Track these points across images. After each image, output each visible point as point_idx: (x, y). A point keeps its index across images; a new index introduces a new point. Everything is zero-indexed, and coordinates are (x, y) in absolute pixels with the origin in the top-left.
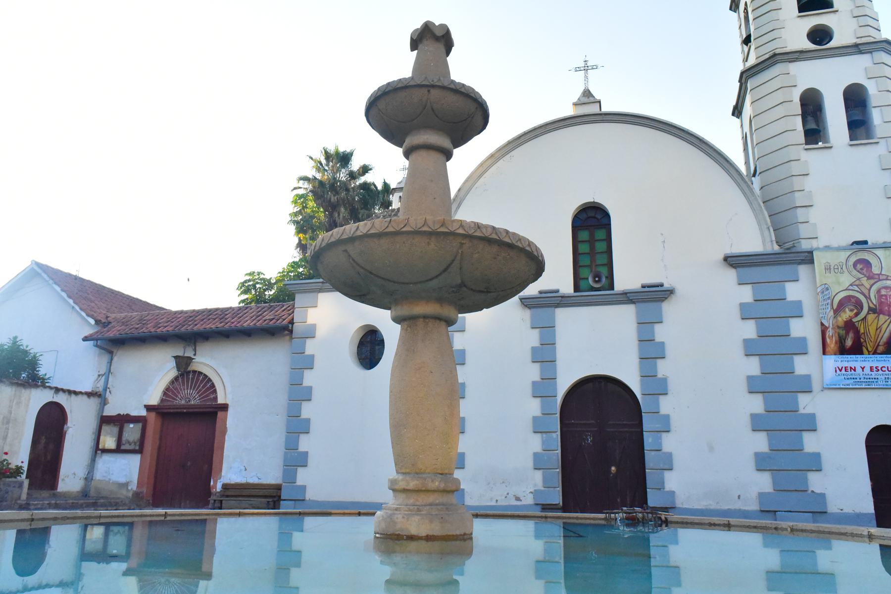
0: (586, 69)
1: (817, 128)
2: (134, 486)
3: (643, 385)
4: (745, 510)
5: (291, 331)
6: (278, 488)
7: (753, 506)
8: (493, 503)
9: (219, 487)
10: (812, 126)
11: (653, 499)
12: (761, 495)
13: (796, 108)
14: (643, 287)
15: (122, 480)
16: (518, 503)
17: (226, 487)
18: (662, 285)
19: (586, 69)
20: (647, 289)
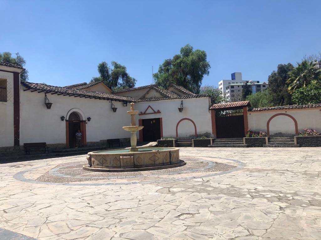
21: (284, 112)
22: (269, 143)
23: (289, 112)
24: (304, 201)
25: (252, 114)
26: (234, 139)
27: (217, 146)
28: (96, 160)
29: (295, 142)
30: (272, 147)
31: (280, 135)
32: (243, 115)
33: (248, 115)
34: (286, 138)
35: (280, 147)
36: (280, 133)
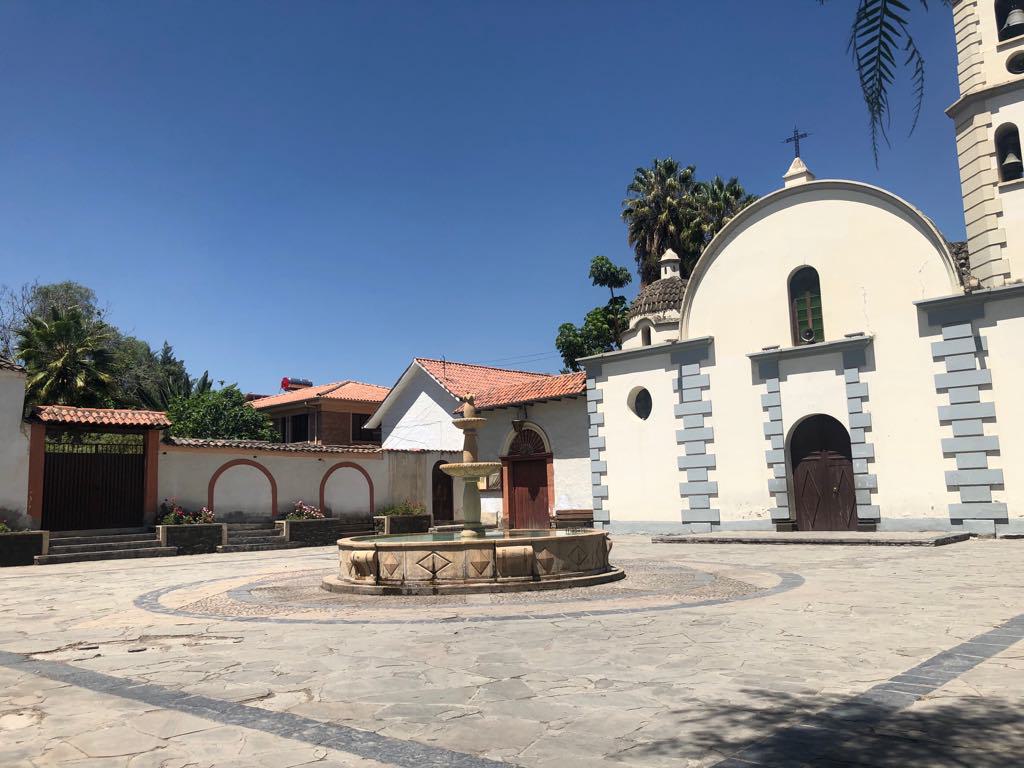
0: (796, 138)
1: (1018, 161)
2: (501, 515)
3: (851, 421)
4: (938, 519)
5: (586, 395)
6: (590, 513)
7: (947, 516)
8: (741, 520)
9: (554, 515)
10: (1011, 159)
11: (862, 513)
12: (951, 506)
13: (991, 146)
14: (847, 336)
15: (495, 511)
16: (758, 519)
17: (559, 513)
18: (861, 334)
19: (796, 138)
20: (849, 339)
21: (251, 458)
22: (231, 539)
23: (261, 459)
24: (698, 599)
25: (173, 453)
26: (97, 534)
27: (102, 555)
28: (559, 555)
29: (285, 534)
30: (244, 550)
31: (237, 517)
32: (143, 457)
33: (161, 456)
34: (253, 526)
35: (262, 549)
36: (240, 514)
